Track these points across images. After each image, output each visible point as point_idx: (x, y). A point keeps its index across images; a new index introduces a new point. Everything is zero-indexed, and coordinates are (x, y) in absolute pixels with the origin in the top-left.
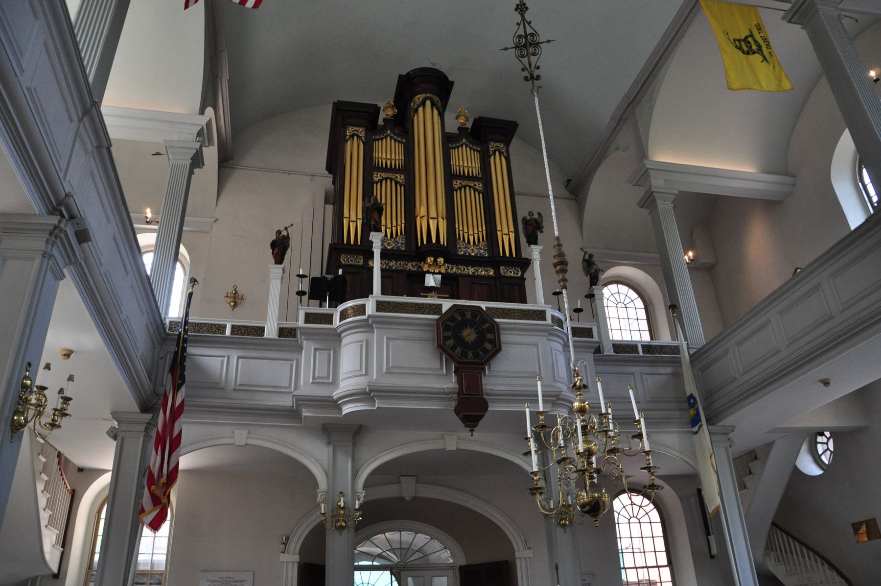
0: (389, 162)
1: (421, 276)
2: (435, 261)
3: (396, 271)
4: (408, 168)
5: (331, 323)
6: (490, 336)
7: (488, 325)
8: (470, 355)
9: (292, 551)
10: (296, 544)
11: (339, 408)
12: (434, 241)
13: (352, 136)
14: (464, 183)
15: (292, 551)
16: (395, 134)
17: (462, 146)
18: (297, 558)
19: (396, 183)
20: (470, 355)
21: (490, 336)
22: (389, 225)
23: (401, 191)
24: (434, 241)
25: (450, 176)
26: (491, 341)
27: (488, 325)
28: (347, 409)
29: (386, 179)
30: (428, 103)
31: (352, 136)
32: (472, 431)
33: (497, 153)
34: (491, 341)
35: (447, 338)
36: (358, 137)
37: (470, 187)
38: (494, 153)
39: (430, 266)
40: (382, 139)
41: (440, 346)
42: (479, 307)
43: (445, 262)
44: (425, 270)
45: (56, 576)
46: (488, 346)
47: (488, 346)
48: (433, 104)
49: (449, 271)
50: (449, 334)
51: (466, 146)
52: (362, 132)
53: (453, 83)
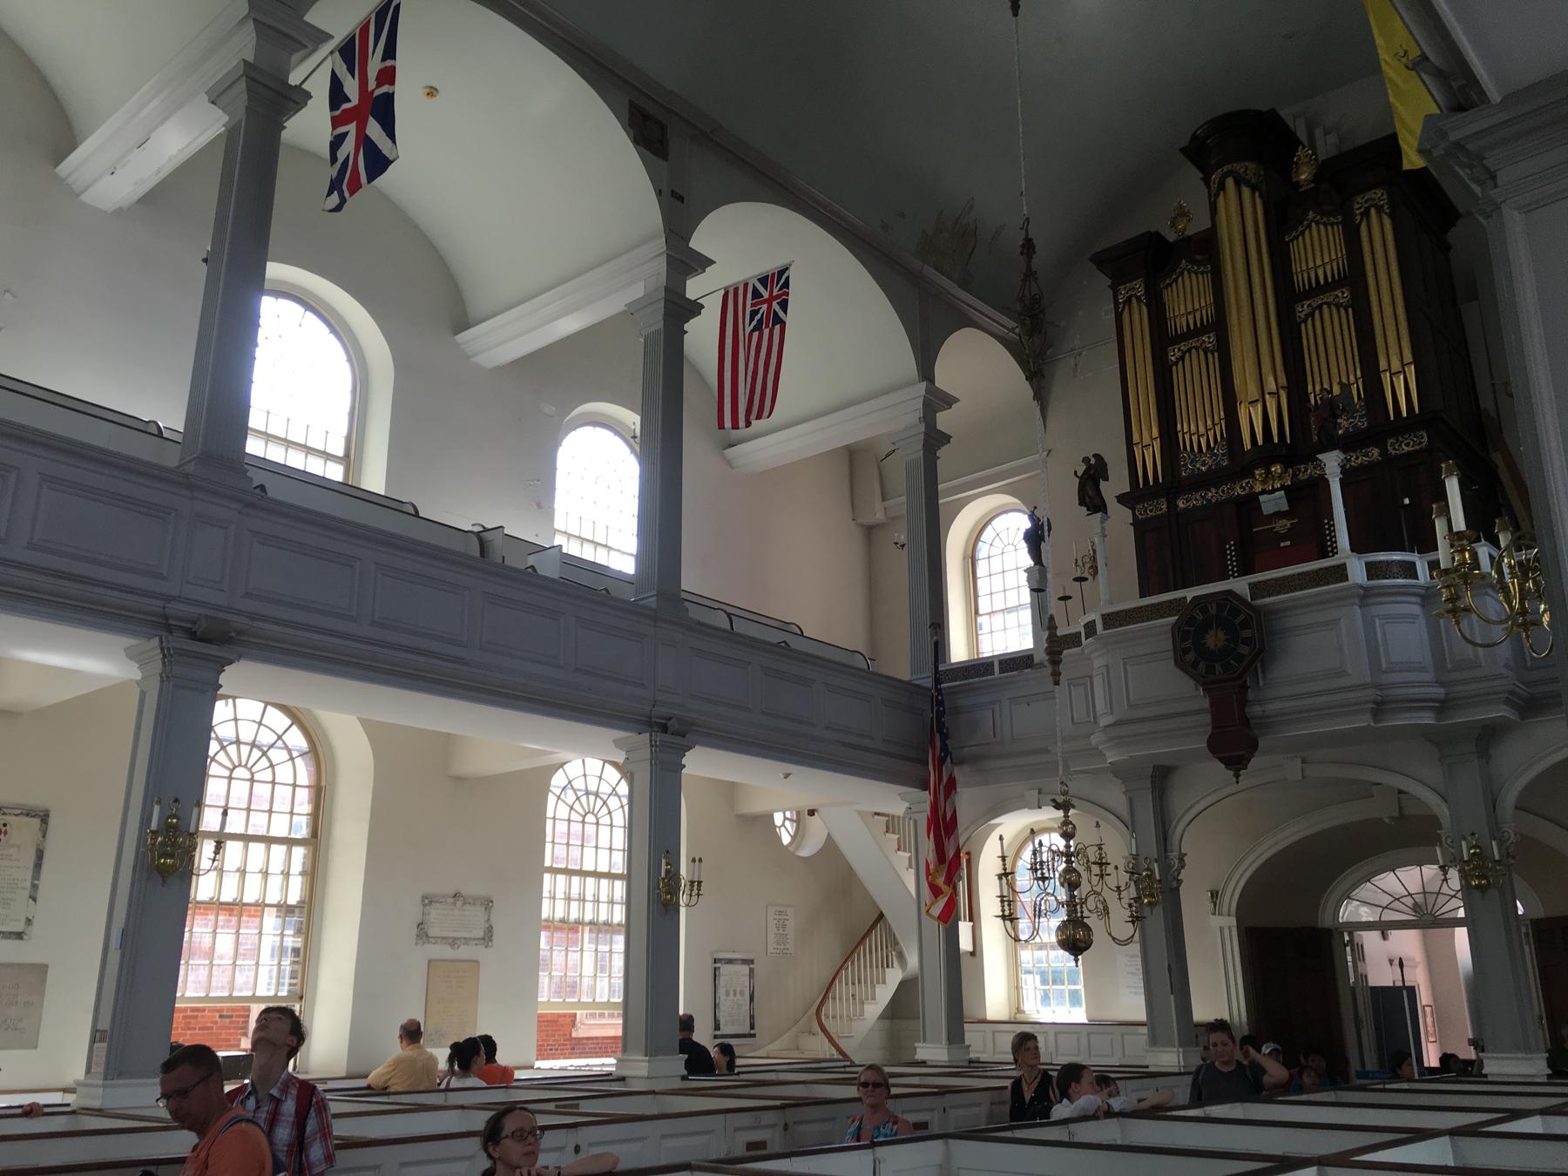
0: (1191, 318)
1: (1253, 499)
2: (1268, 472)
3: (1219, 504)
4: (1218, 325)
5: (1079, 644)
6: (1246, 633)
7: (1242, 617)
8: (1218, 667)
9: (1225, 909)
10: (1231, 899)
11: (1101, 755)
12: (1260, 442)
13: (1129, 300)
14: (1317, 302)
15: (1225, 909)
16: (1194, 262)
17: (1309, 226)
18: (1233, 921)
19: (1206, 351)
20: (1218, 667)
21: (1246, 633)
22: (1202, 430)
23: (1214, 360)
24: (1260, 442)
25: (1289, 296)
26: (1247, 641)
27: (1242, 617)
28: (1112, 757)
29: (1189, 351)
30: (1230, 182)
31: (1129, 300)
32: (1237, 776)
33: (1373, 211)
34: (1247, 641)
35: (1186, 651)
36: (1139, 299)
37: (1329, 304)
38: (1366, 213)
39: (1264, 482)
40: (1176, 280)
41: (1180, 663)
42: (1230, 592)
43: (1285, 471)
44: (1258, 488)
45: (973, 954)
46: (1244, 649)
47: (1244, 649)
48: (1238, 183)
49: (1302, 477)
50: (1188, 644)
51: (1317, 223)
52: (1138, 287)
53: (1273, 112)
